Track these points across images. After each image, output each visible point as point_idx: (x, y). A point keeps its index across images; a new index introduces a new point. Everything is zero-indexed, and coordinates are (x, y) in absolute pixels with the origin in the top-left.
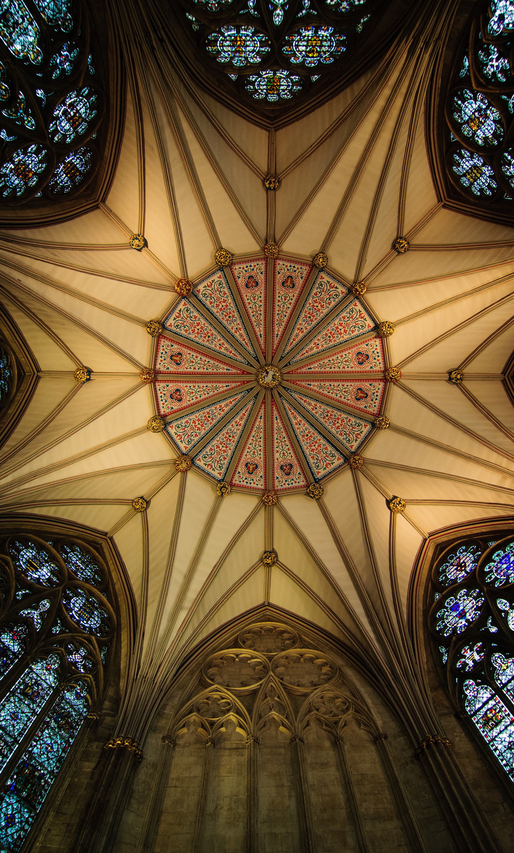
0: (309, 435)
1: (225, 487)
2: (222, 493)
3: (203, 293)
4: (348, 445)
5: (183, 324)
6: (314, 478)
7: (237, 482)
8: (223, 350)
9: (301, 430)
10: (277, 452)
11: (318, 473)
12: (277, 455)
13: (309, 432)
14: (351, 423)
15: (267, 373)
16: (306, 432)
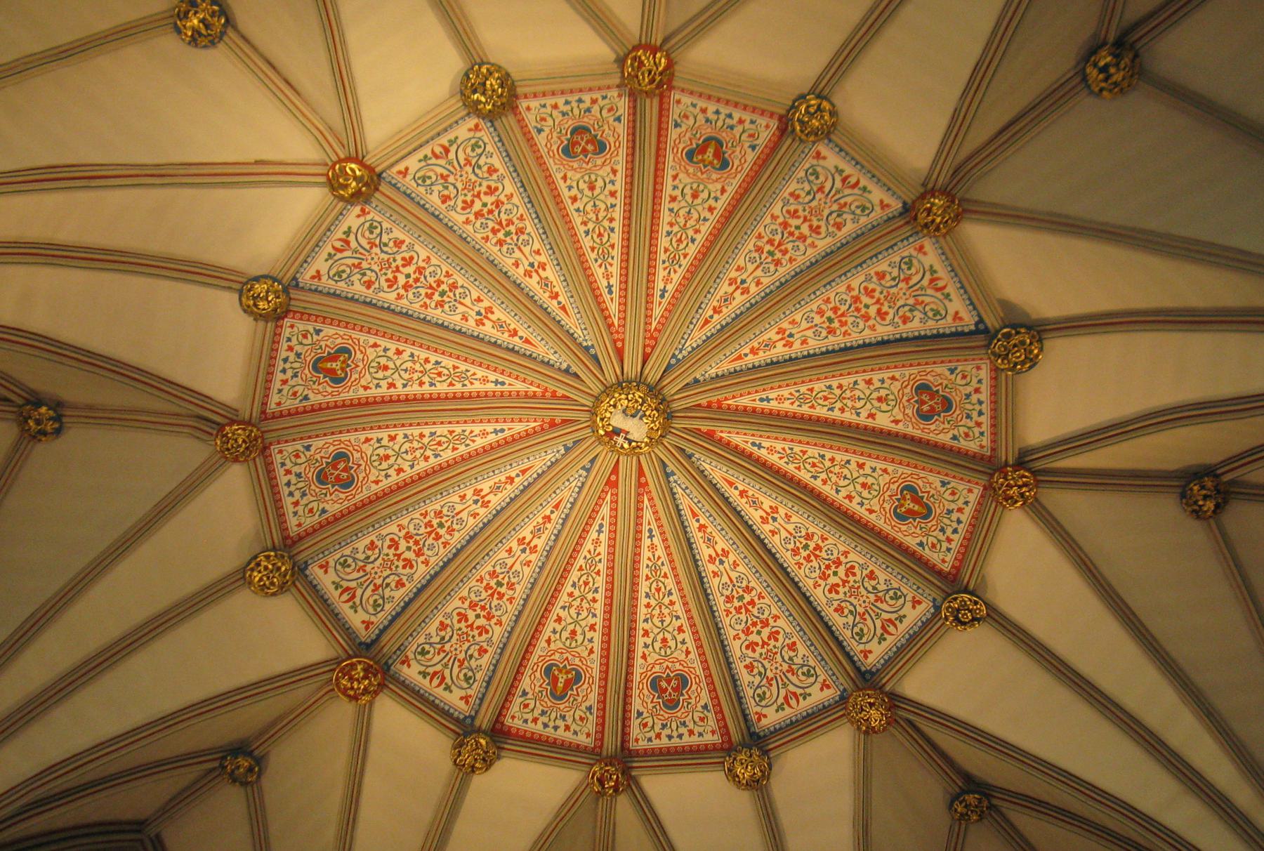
0: (830, 314)
1: (958, 610)
2: (974, 619)
3: (371, 610)
4: (877, 214)
5: (461, 663)
6: (971, 333)
7: (949, 557)
8: (540, 543)
9: (810, 333)
10: (872, 416)
11: (956, 316)
12: (883, 421)
13: (821, 312)
14: (803, 194)
15: (617, 432)
16: (817, 320)
